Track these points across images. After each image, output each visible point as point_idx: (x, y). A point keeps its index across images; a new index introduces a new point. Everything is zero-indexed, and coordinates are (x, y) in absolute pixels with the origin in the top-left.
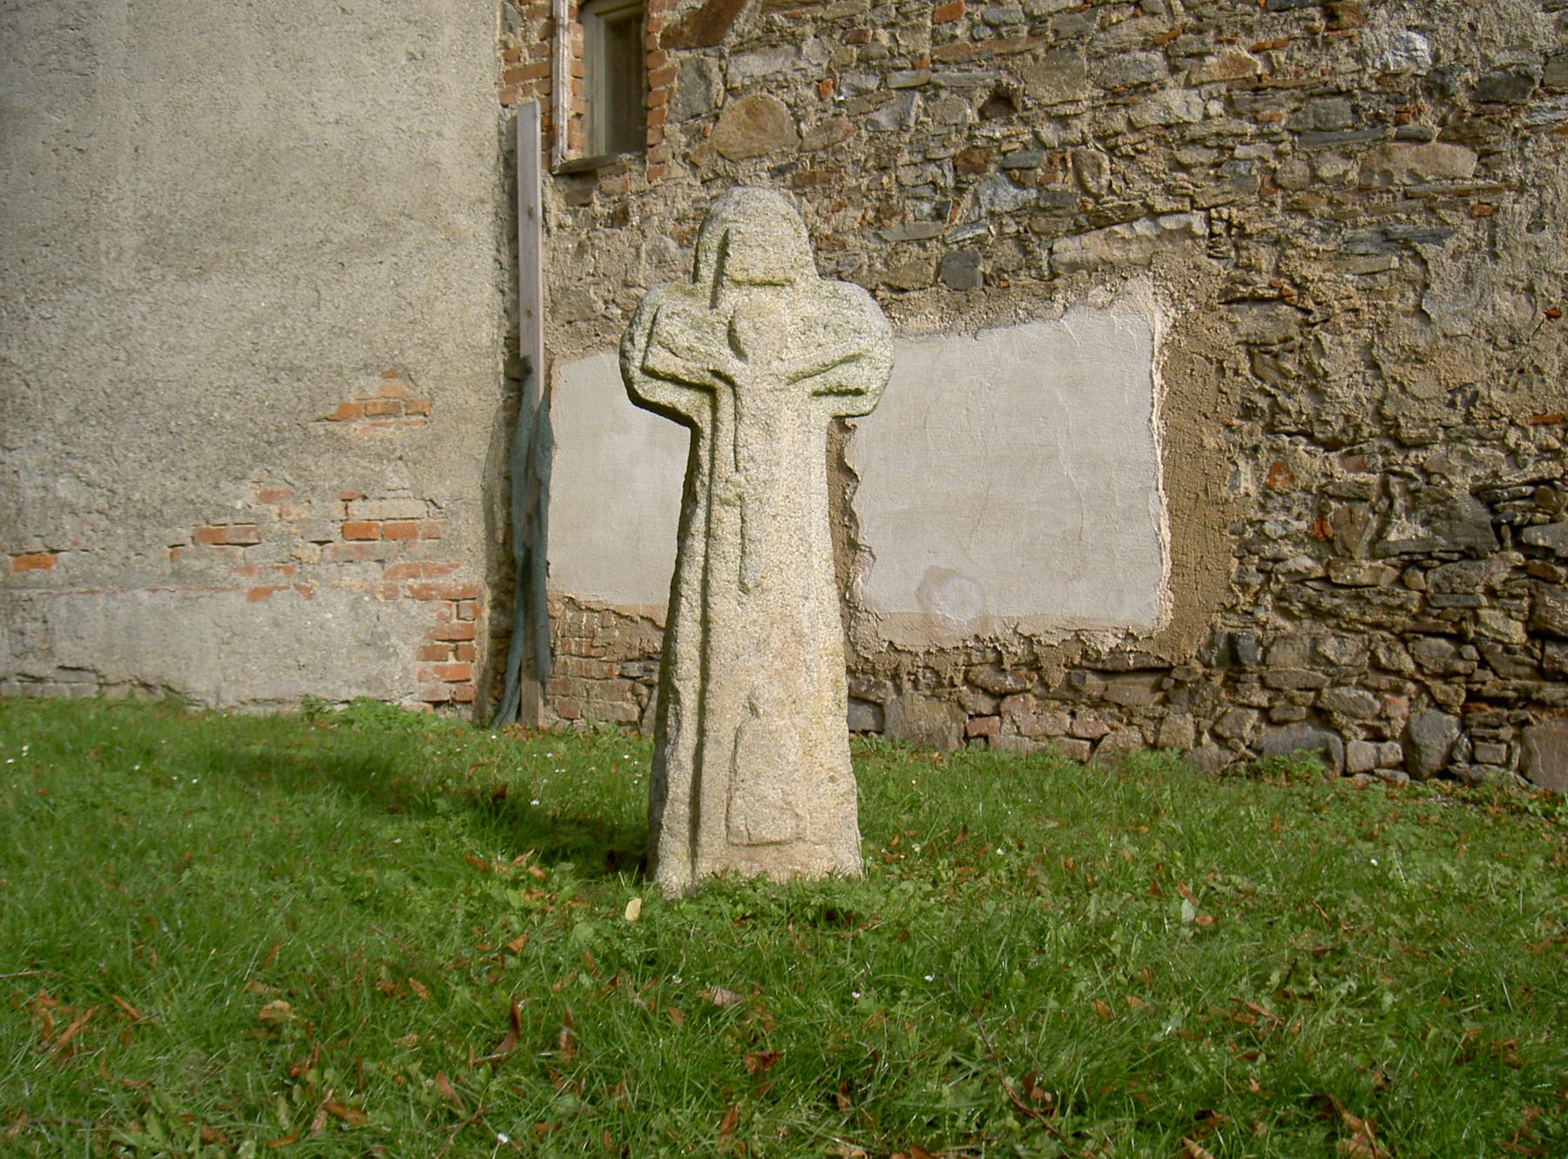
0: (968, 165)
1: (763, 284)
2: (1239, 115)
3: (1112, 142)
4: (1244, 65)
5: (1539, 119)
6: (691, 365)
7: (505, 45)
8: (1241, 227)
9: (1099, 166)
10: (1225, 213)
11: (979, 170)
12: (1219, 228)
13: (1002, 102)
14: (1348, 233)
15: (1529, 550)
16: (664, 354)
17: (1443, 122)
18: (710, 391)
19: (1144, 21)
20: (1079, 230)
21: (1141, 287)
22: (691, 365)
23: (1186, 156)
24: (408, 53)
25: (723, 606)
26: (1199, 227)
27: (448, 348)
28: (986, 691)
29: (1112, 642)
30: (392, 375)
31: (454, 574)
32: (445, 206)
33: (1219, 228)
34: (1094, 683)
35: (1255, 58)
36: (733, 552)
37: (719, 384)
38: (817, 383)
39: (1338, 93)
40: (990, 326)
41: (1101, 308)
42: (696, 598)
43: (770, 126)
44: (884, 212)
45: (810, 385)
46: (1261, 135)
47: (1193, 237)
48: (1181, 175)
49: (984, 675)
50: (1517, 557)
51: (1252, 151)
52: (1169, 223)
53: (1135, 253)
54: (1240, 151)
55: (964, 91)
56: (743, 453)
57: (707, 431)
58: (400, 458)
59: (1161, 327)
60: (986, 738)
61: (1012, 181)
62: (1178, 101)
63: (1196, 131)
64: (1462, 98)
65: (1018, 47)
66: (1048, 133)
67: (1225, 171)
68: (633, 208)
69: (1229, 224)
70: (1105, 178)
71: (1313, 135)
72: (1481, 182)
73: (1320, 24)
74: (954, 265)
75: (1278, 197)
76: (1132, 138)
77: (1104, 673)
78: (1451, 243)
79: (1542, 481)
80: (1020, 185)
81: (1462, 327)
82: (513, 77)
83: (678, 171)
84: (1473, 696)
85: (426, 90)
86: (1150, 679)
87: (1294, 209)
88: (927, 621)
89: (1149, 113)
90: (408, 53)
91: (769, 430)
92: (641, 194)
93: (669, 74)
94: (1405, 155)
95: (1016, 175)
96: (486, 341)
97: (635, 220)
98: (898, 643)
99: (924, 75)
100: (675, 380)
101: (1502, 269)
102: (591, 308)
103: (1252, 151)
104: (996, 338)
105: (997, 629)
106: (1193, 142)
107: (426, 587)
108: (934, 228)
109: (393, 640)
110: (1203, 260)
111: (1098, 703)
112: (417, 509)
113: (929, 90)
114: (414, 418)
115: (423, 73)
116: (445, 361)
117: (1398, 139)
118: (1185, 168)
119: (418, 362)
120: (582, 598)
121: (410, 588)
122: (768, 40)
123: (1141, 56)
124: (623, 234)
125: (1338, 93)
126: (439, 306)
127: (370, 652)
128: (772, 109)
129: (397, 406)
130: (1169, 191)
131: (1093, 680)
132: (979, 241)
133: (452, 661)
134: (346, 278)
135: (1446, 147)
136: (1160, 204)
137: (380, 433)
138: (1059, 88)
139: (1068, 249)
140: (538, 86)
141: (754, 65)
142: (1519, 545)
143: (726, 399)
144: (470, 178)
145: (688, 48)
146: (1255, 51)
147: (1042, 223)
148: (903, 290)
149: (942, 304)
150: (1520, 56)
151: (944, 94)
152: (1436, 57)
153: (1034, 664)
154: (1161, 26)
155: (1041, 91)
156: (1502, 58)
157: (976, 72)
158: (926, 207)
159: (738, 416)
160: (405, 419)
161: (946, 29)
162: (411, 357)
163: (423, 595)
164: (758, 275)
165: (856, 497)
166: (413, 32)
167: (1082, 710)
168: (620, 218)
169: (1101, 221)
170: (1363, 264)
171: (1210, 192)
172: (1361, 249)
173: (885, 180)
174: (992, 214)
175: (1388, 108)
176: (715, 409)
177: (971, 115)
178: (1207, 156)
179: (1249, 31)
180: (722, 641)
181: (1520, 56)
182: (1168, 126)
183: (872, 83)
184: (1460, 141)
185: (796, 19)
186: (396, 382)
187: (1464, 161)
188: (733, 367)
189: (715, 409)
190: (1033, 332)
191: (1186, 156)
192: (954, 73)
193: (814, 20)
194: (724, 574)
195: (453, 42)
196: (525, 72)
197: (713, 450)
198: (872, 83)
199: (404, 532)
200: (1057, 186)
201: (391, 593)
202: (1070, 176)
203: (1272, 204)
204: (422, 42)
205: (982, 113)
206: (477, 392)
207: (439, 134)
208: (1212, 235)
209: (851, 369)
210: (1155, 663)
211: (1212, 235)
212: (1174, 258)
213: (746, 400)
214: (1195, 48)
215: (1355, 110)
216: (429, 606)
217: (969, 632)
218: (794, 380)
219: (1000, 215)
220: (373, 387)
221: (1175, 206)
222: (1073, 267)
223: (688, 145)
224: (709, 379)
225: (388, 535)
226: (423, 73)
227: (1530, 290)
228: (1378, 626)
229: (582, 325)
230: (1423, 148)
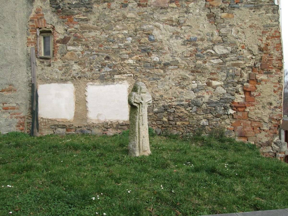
0: (103, 65)
2: (137, 64)
3: (122, 65)
4: (138, 58)
5: (170, 68)
7: (27, 38)
8: (137, 76)
9: (120, 67)
10: (136, 74)
11: (105, 66)
12: (135, 76)
13: (108, 58)
14: (149, 78)
15: (168, 112)
17: (160, 67)
18: (139, 104)
19: (126, 51)
20: (118, 74)
21: (125, 82)
23: (131, 67)
24: (12, 36)
25: (141, 127)
26: (133, 76)
27: (20, 82)
28: (106, 128)
30: (10, 85)
31: (21, 114)
32: (19, 60)
33: (135, 76)
34: (120, 127)
35: (139, 57)
36: (141, 121)
38: (147, 103)
39: (149, 62)
40: (106, 85)
41: (121, 84)
42: (138, 126)
43: (74, 56)
44: (92, 70)
46: (140, 66)
47: (132, 77)
48: (130, 69)
49: (105, 126)
50: (167, 112)
51: (139, 68)
52: (129, 75)
53: (125, 78)
54: (137, 68)
55: (103, 56)
56: (142, 110)
59: (128, 86)
60: (106, 134)
61: (109, 68)
62: (131, 61)
63: (132, 65)
64: (162, 65)
65: (110, 52)
66: (114, 62)
67: (136, 69)
68: (52, 64)
69: (136, 75)
70: (121, 69)
71: (146, 67)
72: (164, 74)
73: (147, 55)
74: (101, 77)
75: (142, 73)
76: (124, 64)
78: (160, 80)
79: (169, 105)
80: (110, 68)
81: (161, 89)
82: (29, 42)
83: (59, 60)
84: (162, 127)
85: (15, 43)
86: (127, 126)
87: (144, 75)
88: (98, 120)
89: (126, 62)
90: (12, 36)
91: (144, 108)
92: (53, 63)
93: (58, 47)
94: (156, 70)
95: (110, 67)
96: (25, 81)
97: (52, 66)
98: (94, 122)
99: (97, 53)
100: (136, 103)
101: (166, 83)
102: (44, 78)
103: (139, 68)
104: (107, 87)
105: (107, 121)
106: (132, 66)
107: (17, 116)
108: (98, 72)
109: (12, 124)
110: (133, 79)
112: (15, 105)
113: (98, 55)
114: (14, 92)
115: (15, 40)
117: (155, 68)
118: (131, 69)
119: (15, 83)
120: (44, 117)
122: (74, 45)
123: (126, 55)
124: (50, 68)
125: (149, 62)
126: (18, 75)
127: (8, 126)
128: (75, 54)
130: (129, 71)
131: (119, 126)
132: (104, 74)
133: (21, 127)
134: (3, 70)
135: (160, 70)
136: (128, 73)
137: (9, 94)
138: (115, 57)
139: (116, 77)
140: (34, 45)
141: (70, 48)
142: (167, 111)
144: (21, 57)
145: (60, 44)
146: (139, 57)
147: (113, 73)
150: (168, 61)
151: (100, 56)
152: (160, 60)
153: (112, 124)
154: (128, 52)
155: (113, 57)
156: (166, 61)
157: (104, 54)
158: (97, 70)
159: (142, 107)
160: (13, 92)
161: (100, 48)
162: (14, 83)
163: (17, 118)
164: (144, 92)
165: (88, 105)
166: (13, 33)
167: (118, 130)
168: (50, 65)
169: (120, 74)
170: (151, 81)
171: (134, 72)
172: (151, 80)
173: (91, 65)
174: (106, 71)
175: (155, 65)
176: (140, 106)
177: (103, 59)
178: (133, 68)
179: (139, 54)
180: (141, 130)
181: (168, 61)
182: (129, 64)
183: (90, 53)
184: (162, 69)
185: (78, 43)
186: (11, 86)
187: (162, 71)
188: (142, 102)
189: (140, 106)
190: (112, 86)
191: (131, 67)
192: (101, 53)
193: (81, 43)
195: (19, 36)
196: (31, 42)
197: (139, 110)
198: (90, 53)
199: (13, 108)
200: (115, 69)
201: (11, 118)
202: (117, 68)
203: (141, 74)
204: (14, 35)
205: (105, 59)
206: (24, 88)
207: (18, 50)
208: (134, 76)
210: (127, 124)
211: (134, 76)
212: (129, 79)
214: (132, 55)
215: (150, 65)
216: (17, 119)
217: (104, 121)
219: (107, 72)
220: (7, 87)
221: (130, 73)
222: (117, 79)
223: (61, 57)
224: (139, 103)
225: (11, 109)
226: (15, 40)
227: (169, 85)
228: (153, 120)
229: (43, 80)
230: (158, 70)
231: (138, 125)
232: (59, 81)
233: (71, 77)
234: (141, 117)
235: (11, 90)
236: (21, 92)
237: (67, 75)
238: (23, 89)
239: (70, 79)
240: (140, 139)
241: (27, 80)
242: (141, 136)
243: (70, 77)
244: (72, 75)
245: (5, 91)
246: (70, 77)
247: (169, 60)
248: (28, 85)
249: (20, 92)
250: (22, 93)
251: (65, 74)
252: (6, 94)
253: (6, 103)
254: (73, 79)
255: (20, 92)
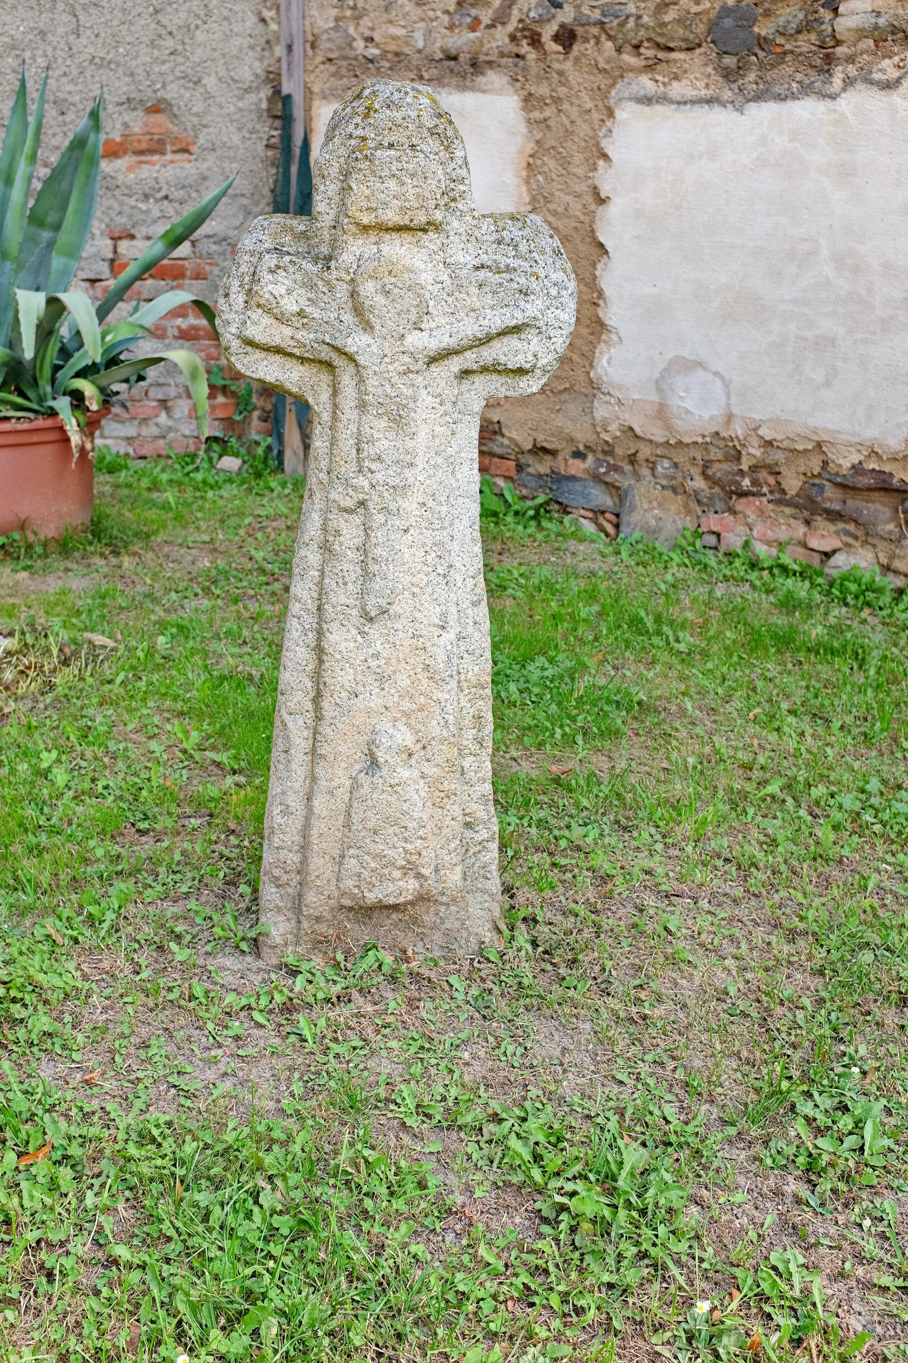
1: (399, 229)
6: (301, 335)
16: (267, 320)
18: (329, 366)
22: (301, 335)
25: (340, 639)
27: (210, 82)
29: (856, 458)
30: (155, 109)
34: (831, 497)
36: (352, 571)
37: (338, 361)
40: (758, 97)
45: (455, 364)
56: (369, 450)
57: (326, 417)
58: (166, 197)
60: (718, 535)
74: (728, 23)
77: (843, 486)
91: (398, 420)
104: (763, 113)
105: (739, 430)
111: (834, 516)
114: (178, 157)
116: (208, 96)
121: (179, 327)
126: (200, 36)
129: (161, 142)
131: (830, 491)
137: (145, 172)
143: (347, 380)
148: (671, 49)
149: (710, 70)
159: (362, 406)
160: (169, 157)
162: (172, 92)
164: (391, 216)
180: (341, 677)
186: (160, 118)
188: (357, 342)
190: (806, 110)
194: (341, 597)
197: (333, 442)
206: (239, 129)
209: (512, 342)
213: (372, 383)
218: (433, 360)
220: (137, 122)
224: (325, 353)
231: (312, 605)
232: (434, 72)
233: (513, 38)
234: (350, 531)
235: (161, 142)
236: (221, 159)
237: (486, 20)
238: (236, 139)
239: (502, 55)
240: (320, 772)
241: (259, 68)
242: (343, 747)
243: (501, 36)
244: (515, 14)
245: (125, 152)
246: (501, 36)
248: (264, 105)
249: (210, 162)
250: (226, 165)
251: (474, 12)
252: (130, 169)
253: (132, 237)
254: (525, 48)
255: (211, 158)
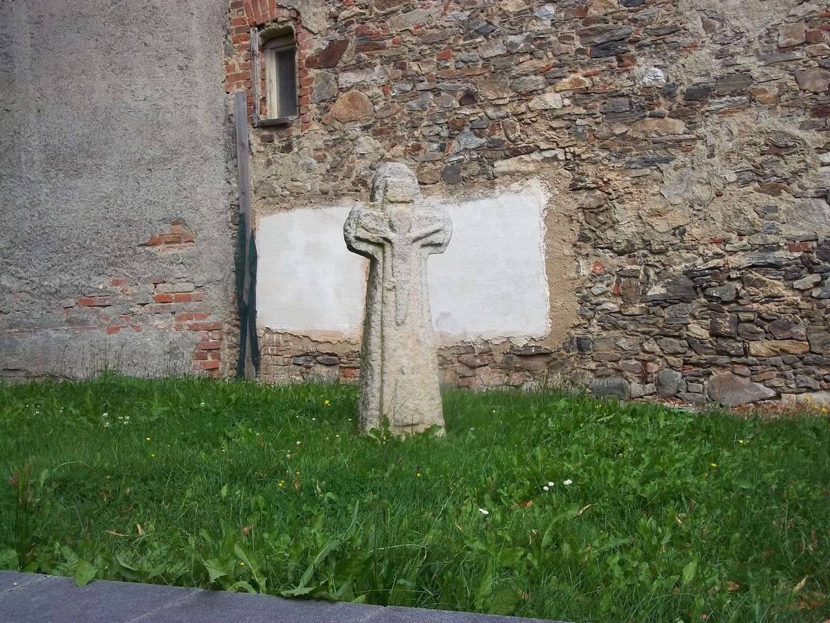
0: (456, 128)
1: (402, 202)
2: (579, 105)
3: (521, 117)
4: (581, 82)
5: (712, 108)
6: (374, 235)
7: (227, 63)
8: (579, 155)
9: (515, 128)
10: (572, 149)
11: (461, 130)
12: (569, 156)
13: (469, 98)
14: (627, 159)
15: (710, 298)
16: (363, 231)
17: (670, 109)
18: (381, 245)
19: (535, 62)
20: (507, 157)
21: (534, 182)
22: (374, 235)
23: (555, 124)
24: (179, 66)
25: (389, 331)
26: (561, 157)
27: (204, 210)
28: (467, 365)
29: (525, 342)
34: (518, 362)
37: (385, 243)
39: (623, 95)
42: (378, 328)
43: (360, 106)
45: (420, 243)
46: (589, 115)
47: (558, 160)
48: (552, 132)
49: (465, 358)
50: (703, 300)
52: (548, 154)
53: (531, 167)
54: (579, 122)
55: (452, 92)
57: (381, 261)
58: (182, 263)
59: (544, 201)
61: (476, 135)
62: (552, 99)
63: (559, 113)
64: (680, 99)
65: (478, 73)
66: (490, 112)
68: (294, 143)
69: (573, 153)
71: (612, 115)
72: (687, 136)
73: (615, 64)
74: (449, 172)
76: (529, 115)
77: (521, 356)
78: (673, 163)
79: (715, 268)
80: (480, 136)
81: (679, 200)
82: (232, 79)
83: (315, 126)
84: (685, 363)
85: (189, 85)
87: (604, 148)
89: (535, 103)
90: (179, 66)
92: (298, 137)
93: (310, 80)
94: (652, 124)
97: (296, 149)
99: (434, 85)
100: (367, 241)
101: (696, 175)
103: (584, 122)
106: (558, 117)
108: (439, 155)
111: (517, 370)
112: (190, 287)
113: (436, 92)
116: (202, 216)
117: (650, 116)
118: (554, 129)
120: (273, 328)
121: (188, 325)
122: (359, 66)
123: (533, 77)
124: (289, 155)
125: (623, 95)
126: (199, 190)
128: (361, 99)
129: (179, 238)
131: (516, 359)
132: (460, 161)
133: (210, 359)
135: (671, 120)
136: (543, 146)
138: (495, 92)
139: (502, 166)
140: (245, 84)
141: (349, 78)
142: (705, 296)
143: (388, 249)
144: (209, 128)
147: (489, 154)
148: (425, 184)
149: (443, 191)
150: (704, 79)
151: (443, 94)
152: (668, 80)
155: (487, 93)
156: (697, 80)
157: (458, 84)
158: (435, 146)
159: (393, 256)
160: (183, 244)
161: (442, 63)
162: (186, 215)
163: (194, 328)
164: (400, 199)
166: (181, 56)
168: (288, 148)
169: (516, 153)
170: (634, 173)
171: (565, 139)
172: (633, 166)
173: (416, 133)
174: (466, 149)
176: (384, 252)
179: (583, 66)
180: (390, 345)
181: (704, 79)
182: (546, 110)
183: (409, 87)
184: (678, 117)
187: (679, 126)
188: (391, 235)
190: (485, 203)
191: (555, 124)
192: (447, 84)
193: (381, 57)
194: (389, 318)
196: (237, 77)
197: (384, 268)
198: (409, 87)
199: (186, 298)
200: (496, 137)
201: (179, 328)
202: (503, 132)
203: (593, 145)
204: (186, 61)
207: (196, 107)
209: (437, 235)
210: (543, 350)
211: (566, 159)
212: (549, 170)
214: (558, 74)
215: (631, 104)
218: (414, 241)
220: (167, 229)
222: (504, 174)
223: (321, 114)
224: (381, 241)
225: (178, 300)
227: (709, 183)
228: (644, 333)
230: (661, 121)
231: (379, 323)
232: (317, 200)
233: (353, 183)
234: (391, 296)
235: (179, 238)
236: (209, 244)
237: (341, 177)
238: (216, 235)
239: (349, 190)
240: (385, 378)
241: (227, 203)
242: (391, 367)
243: (348, 183)
244: (354, 174)
245: (161, 244)
246: (348, 183)
247: (708, 75)
248: (230, 219)
249: (204, 246)
250: (212, 248)
251: (334, 174)
252: (164, 250)
253: (164, 282)
254: (360, 187)
255: (205, 243)
